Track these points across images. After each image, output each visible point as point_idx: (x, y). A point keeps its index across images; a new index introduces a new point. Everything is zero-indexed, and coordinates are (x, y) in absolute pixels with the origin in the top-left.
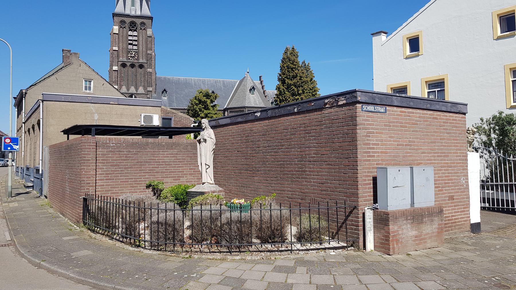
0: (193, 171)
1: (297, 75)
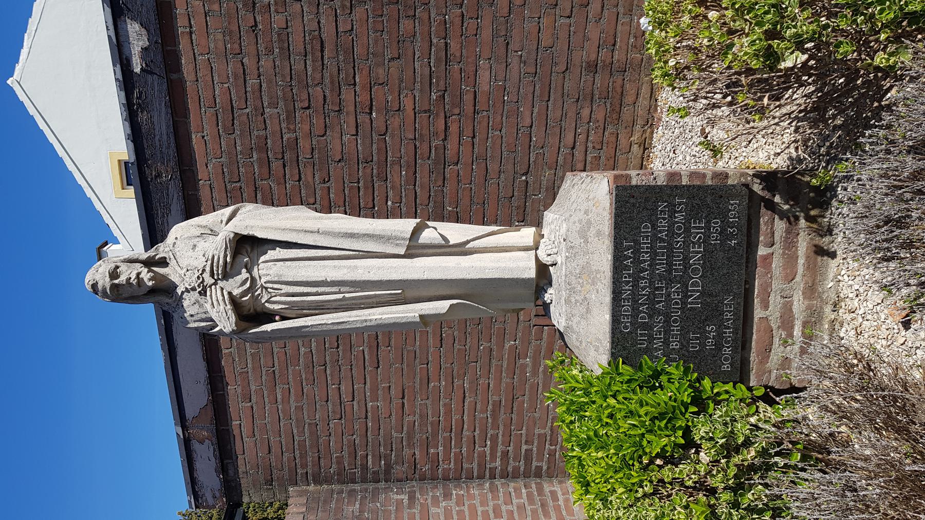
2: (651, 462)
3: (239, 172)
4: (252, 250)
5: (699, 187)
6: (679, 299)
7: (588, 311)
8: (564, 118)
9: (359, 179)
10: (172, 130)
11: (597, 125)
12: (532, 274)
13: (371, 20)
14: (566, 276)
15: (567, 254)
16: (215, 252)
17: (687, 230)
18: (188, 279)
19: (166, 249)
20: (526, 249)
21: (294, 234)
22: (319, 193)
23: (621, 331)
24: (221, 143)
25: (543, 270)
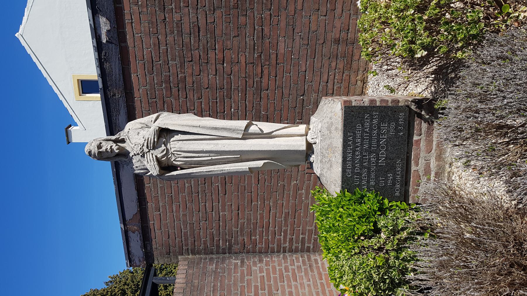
0: (261, 290)
1: (122, 290)
2: (359, 238)
3: (155, 94)
4: (167, 135)
5: (385, 107)
6: (374, 161)
7: (331, 166)
8: (322, 67)
9: (217, 97)
10: (121, 72)
11: (340, 71)
12: (304, 148)
13: (224, 17)
14: (321, 149)
15: (321, 138)
16: (149, 136)
17: (379, 128)
18: (135, 149)
19: (124, 135)
20: (302, 135)
21: (188, 128)
22: (196, 104)
23: (346, 176)
24: (146, 79)
25: (310, 146)
